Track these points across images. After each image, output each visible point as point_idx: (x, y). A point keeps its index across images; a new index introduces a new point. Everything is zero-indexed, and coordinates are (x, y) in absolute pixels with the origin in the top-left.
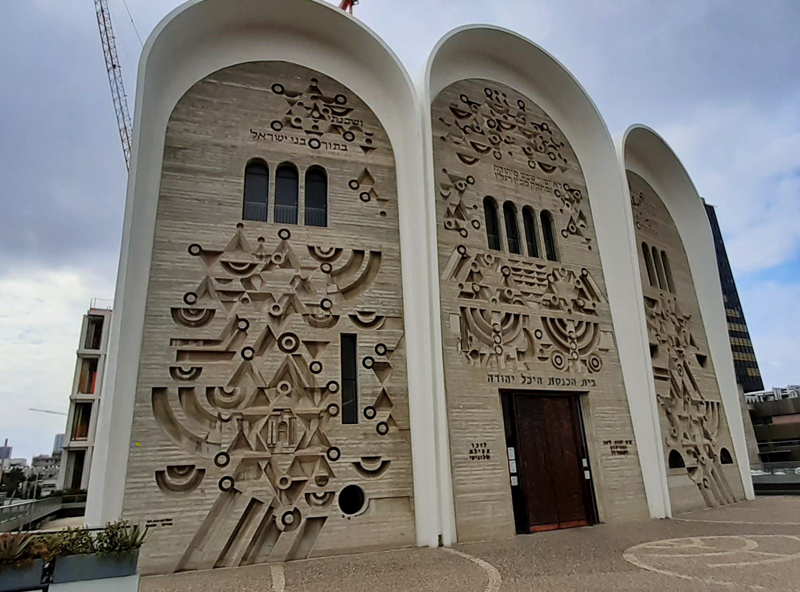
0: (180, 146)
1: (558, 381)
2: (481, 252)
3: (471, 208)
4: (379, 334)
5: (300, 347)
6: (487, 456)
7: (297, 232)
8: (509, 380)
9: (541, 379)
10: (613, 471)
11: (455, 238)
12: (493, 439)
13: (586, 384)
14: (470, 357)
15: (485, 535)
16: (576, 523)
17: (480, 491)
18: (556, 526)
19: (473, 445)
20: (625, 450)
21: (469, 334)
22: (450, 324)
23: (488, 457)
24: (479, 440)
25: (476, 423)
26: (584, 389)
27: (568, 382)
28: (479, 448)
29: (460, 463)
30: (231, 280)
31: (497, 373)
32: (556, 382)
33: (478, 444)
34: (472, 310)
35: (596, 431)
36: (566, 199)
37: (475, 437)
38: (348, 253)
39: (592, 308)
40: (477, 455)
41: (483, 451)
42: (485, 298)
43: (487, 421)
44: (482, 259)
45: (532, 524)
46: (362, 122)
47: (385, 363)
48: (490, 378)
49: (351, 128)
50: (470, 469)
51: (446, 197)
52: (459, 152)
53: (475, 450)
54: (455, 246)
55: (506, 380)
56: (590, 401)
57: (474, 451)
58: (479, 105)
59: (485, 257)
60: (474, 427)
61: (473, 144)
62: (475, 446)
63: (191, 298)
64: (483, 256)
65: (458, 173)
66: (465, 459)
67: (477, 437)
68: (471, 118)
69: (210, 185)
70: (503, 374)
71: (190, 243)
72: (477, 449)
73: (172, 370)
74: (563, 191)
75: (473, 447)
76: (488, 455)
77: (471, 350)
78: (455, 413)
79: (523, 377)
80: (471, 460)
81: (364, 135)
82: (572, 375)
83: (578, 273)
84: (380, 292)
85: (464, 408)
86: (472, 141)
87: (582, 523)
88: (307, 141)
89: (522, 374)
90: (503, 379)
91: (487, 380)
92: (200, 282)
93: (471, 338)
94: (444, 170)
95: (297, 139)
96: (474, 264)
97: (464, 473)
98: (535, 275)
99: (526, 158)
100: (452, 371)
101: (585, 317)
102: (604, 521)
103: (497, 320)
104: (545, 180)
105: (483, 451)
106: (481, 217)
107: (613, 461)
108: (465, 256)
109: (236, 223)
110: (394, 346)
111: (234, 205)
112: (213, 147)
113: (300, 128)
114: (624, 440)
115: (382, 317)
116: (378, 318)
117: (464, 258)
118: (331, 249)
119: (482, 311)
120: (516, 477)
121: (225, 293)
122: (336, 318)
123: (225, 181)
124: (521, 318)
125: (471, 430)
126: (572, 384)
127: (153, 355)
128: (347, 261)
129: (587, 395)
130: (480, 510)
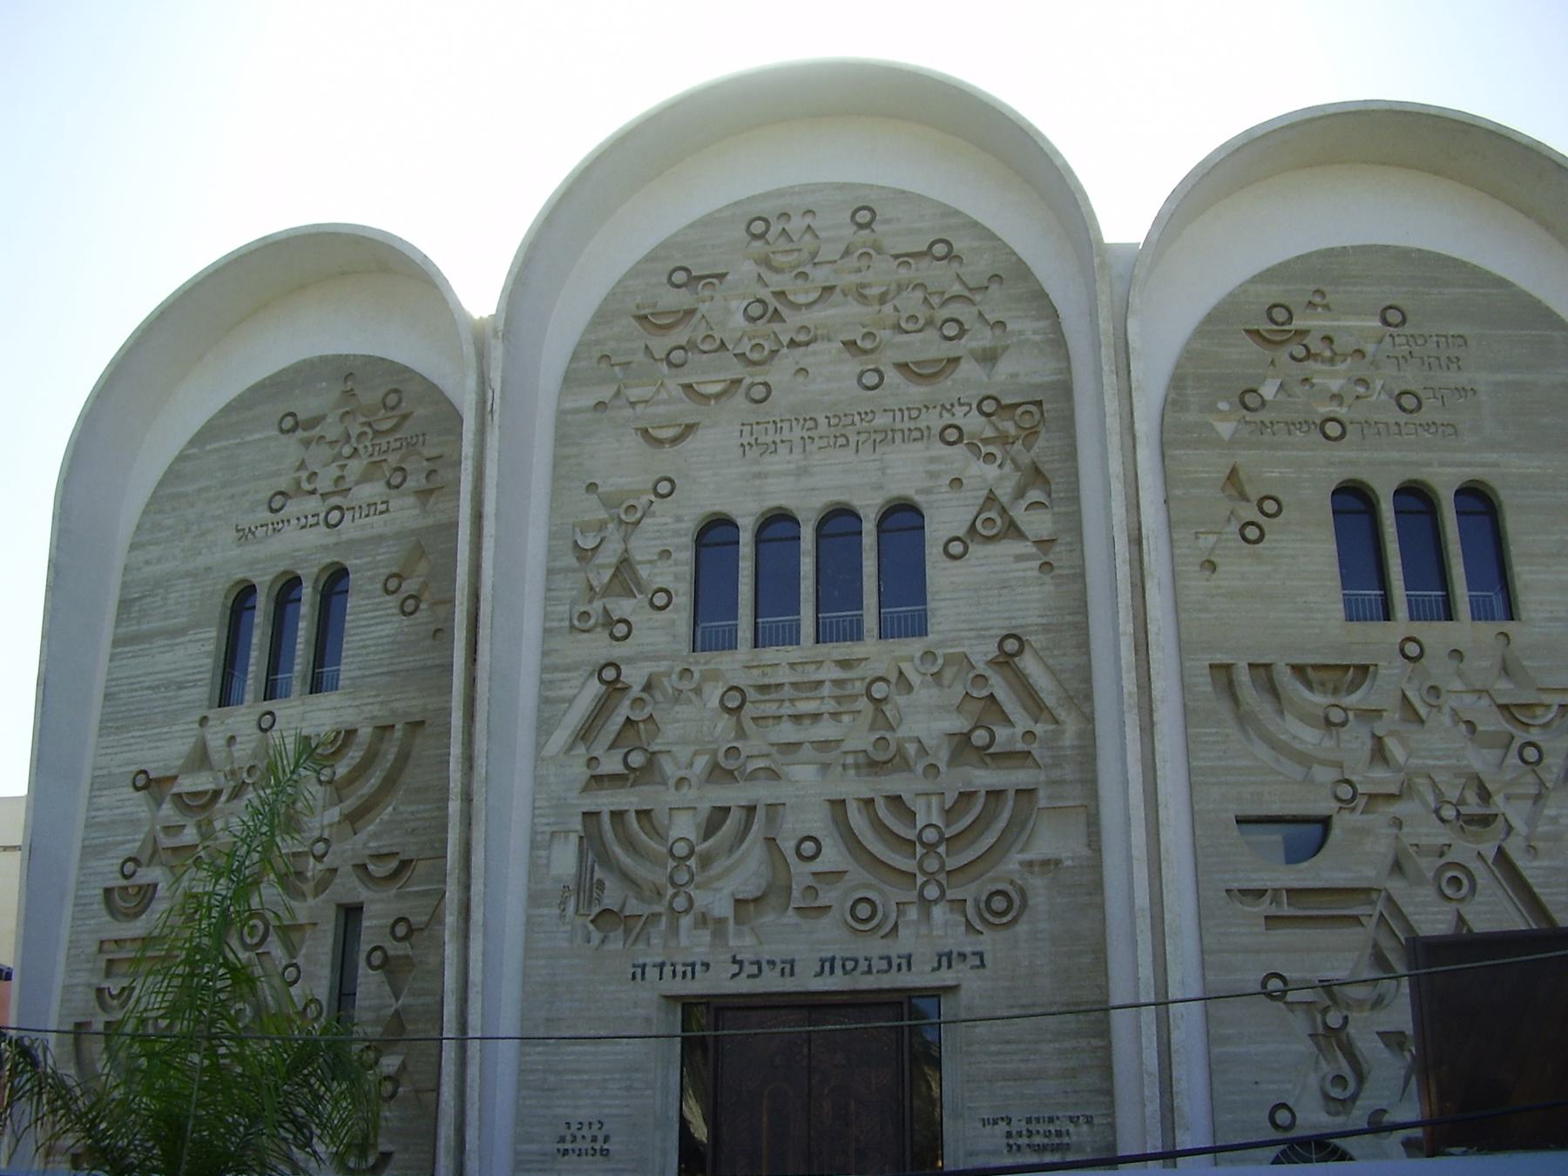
0: (136, 595)
2: (663, 666)
3: (651, 562)
4: (400, 896)
5: (269, 939)
6: (602, 1150)
7: (287, 712)
9: (792, 963)
11: (598, 647)
13: (950, 966)
14: (591, 927)
20: (1066, 1140)
21: (598, 874)
22: (548, 858)
23: (605, 1153)
25: (585, 1077)
26: (946, 977)
27: (884, 965)
28: (585, 1131)
30: (183, 826)
31: (659, 960)
34: (618, 816)
36: (986, 441)
38: (365, 732)
39: (1020, 746)
41: (594, 1139)
42: (664, 783)
44: (665, 680)
46: (424, 434)
47: (407, 957)
48: (639, 971)
49: (403, 459)
51: (584, 555)
52: (642, 424)
54: (590, 669)
57: (569, 1138)
58: (721, 276)
59: (674, 677)
61: (688, 387)
62: (574, 1127)
63: (130, 867)
64: (668, 674)
65: (629, 479)
68: (695, 320)
69: (168, 656)
70: (678, 959)
71: (135, 768)
72: (579, 1134)
73: (100, 991)
74: (973, 423)
75: (569, 1128)
76: (605, 1147)
77: (596, 910)
79: (741, 963)
81: (425, 463)
82: (906, 941)
83: (982, 652)
84: (413, 808)
86: (686, 381)
88: (322, 516)
89: (734, 957)
90: (674, 971)
91: (631, 976)
92: (142, 836)
93: (601, 884)
94: (592, 487)
95: (306, 517)
96: (638, 701)
98: (826, 690)
99: (852, 367)
101: (984, 778)
103: (684, 828)
104: (908, 409)
106: (677, 577)
108: (619, 686)
109: (197, 718)
110: (425, 919)
111: (200, 683)
112: (181, 581)
113: (313, 492)
115: (412, 860)
116: (405, 864)
117: (615, 688)
118: (339, 733)
119: (643, 814)
121: (175, 850)
122: (334, 871)
123: (190, 641)
124: (760, 814)
126: (899, 968)
127: (78, 970)
128: (361, 753)
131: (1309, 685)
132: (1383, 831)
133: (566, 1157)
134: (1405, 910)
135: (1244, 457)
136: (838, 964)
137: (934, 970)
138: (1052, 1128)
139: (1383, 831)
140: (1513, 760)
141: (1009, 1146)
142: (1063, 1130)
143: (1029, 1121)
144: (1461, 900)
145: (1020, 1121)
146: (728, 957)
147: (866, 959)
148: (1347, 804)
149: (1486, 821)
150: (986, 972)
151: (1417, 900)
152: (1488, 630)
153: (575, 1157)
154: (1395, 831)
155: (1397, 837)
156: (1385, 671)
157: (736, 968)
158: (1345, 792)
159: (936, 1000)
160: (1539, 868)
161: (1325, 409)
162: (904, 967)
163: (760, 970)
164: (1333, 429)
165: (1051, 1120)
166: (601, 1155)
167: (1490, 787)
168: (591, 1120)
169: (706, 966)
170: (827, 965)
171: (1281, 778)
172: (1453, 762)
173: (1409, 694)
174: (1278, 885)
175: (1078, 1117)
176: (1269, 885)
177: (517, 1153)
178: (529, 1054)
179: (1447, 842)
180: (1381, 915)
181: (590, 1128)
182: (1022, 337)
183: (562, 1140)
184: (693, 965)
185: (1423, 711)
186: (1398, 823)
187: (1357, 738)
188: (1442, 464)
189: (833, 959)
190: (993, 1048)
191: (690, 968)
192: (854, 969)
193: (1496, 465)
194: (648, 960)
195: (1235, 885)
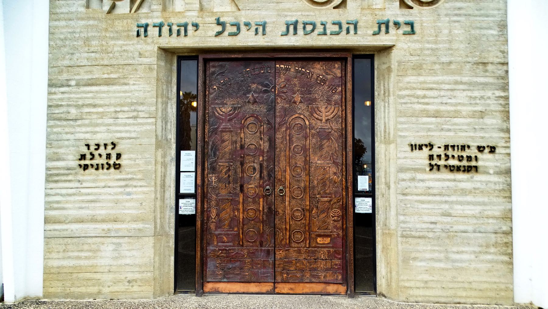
1: (309, 28)
6: (115, 164)
8: (186, 31)
9: (264, 26)
10: (422, 202)
12: (133, 135)
13: (387, 32)
15: (94, 290)
16: (318, 287)
17: (93, 220)
18: (268, 287)
19: (88, 146)
20: (473, 163)
23: (117, 166)
24: (102, 137)
25: (100, 110)
26: (383, 40)
27: (336, 28)
28: (102, 150)
29: (57, 175)
31: (158, 21)
32: (304, 28)
33: (98, 145)
35: (397, 123)
37: (95, 133)
40: (94, 162)
41: (109, 156)
43: (121, 105)
45: (209, 280)
50: (77, 185)
53: (91, 154)
55: (179, 31)
56: (394, 65)
57: (88, 156)
60: (95, 116)
62: (92, 148)
66: (68, 169)
67: (98, 132)
70: (174, 20)
72: (96, 153)
75: (89, 149)
76: (117, 162)
78: (59, 94)
80: (81, 171)
85: (78, 85)
87: (331, 288)
89: (218, 20)
90: (170, 30)
91: (136, 33)
97: (64, 191)
100: (63, 23)
102: (384, 293)
105: (109, 156)
107: (431, 184)
114: (474, 144)
120: (193, 201)
125: (87, 122)
126: (348, 32)
129: (389, 53)
130: (90, 251)
133: (87, 171)
136: (300, 27)
137: (374, 34)
138: (465, 154)
141: (431, 165)
142: (473, 156)
143: (446, 147)
145: (439, 147)
146: (213, 19)
147: (322, 24)
150: (414, 37)
153: (93, 170)
157: (219, 28)
159: (367, 62)
162: (352, 31)
163: (239, 29)
165: (463, 148)
166: (115, 168)
168: (105, 142)
169: (196, 26)
170: (291, 28)
175: (484, 147)
177: (48, 169)
178: (55, 93)
181: (105, 148)
183: (83, 157)
184: (185, 26)
189: (297, 22)
190: (420, 93)
191: (183, 28)
192: (313, 31)
194: (149, 21)
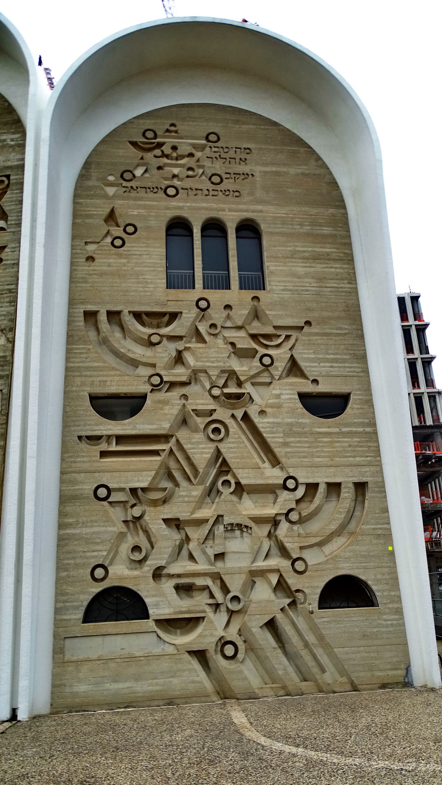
131: (143, 324)
132: (176, 402)
134: (185, 446)
135: (118, 204)
139: (176, 402)
140: (256, 363)
144: (221, 440)
148: (155, 388)
149: (239, 396)
151: (193, 440)
152: (248, 294)
154: (183, 401)
155: (184, 405)
156: (186, 315)
158: (156, 380)
160: (268, 423)
161: (167, 183)
164: (171, 191)
167: (242, 378)
171: (118, 373)
172: (221, 364)
173: (200, 328)
174: (110, 433)
176: (105, 433)
179: (214, 408)
180: (171, 451)
182: (5, 143)
185: (207, 338)
186: (185, 397)
187: (166, 350)
188: (230, 210)
193: (261, 211)
195: (84, 434)
